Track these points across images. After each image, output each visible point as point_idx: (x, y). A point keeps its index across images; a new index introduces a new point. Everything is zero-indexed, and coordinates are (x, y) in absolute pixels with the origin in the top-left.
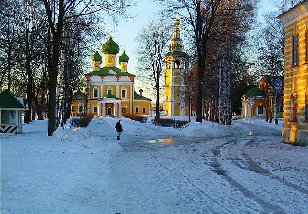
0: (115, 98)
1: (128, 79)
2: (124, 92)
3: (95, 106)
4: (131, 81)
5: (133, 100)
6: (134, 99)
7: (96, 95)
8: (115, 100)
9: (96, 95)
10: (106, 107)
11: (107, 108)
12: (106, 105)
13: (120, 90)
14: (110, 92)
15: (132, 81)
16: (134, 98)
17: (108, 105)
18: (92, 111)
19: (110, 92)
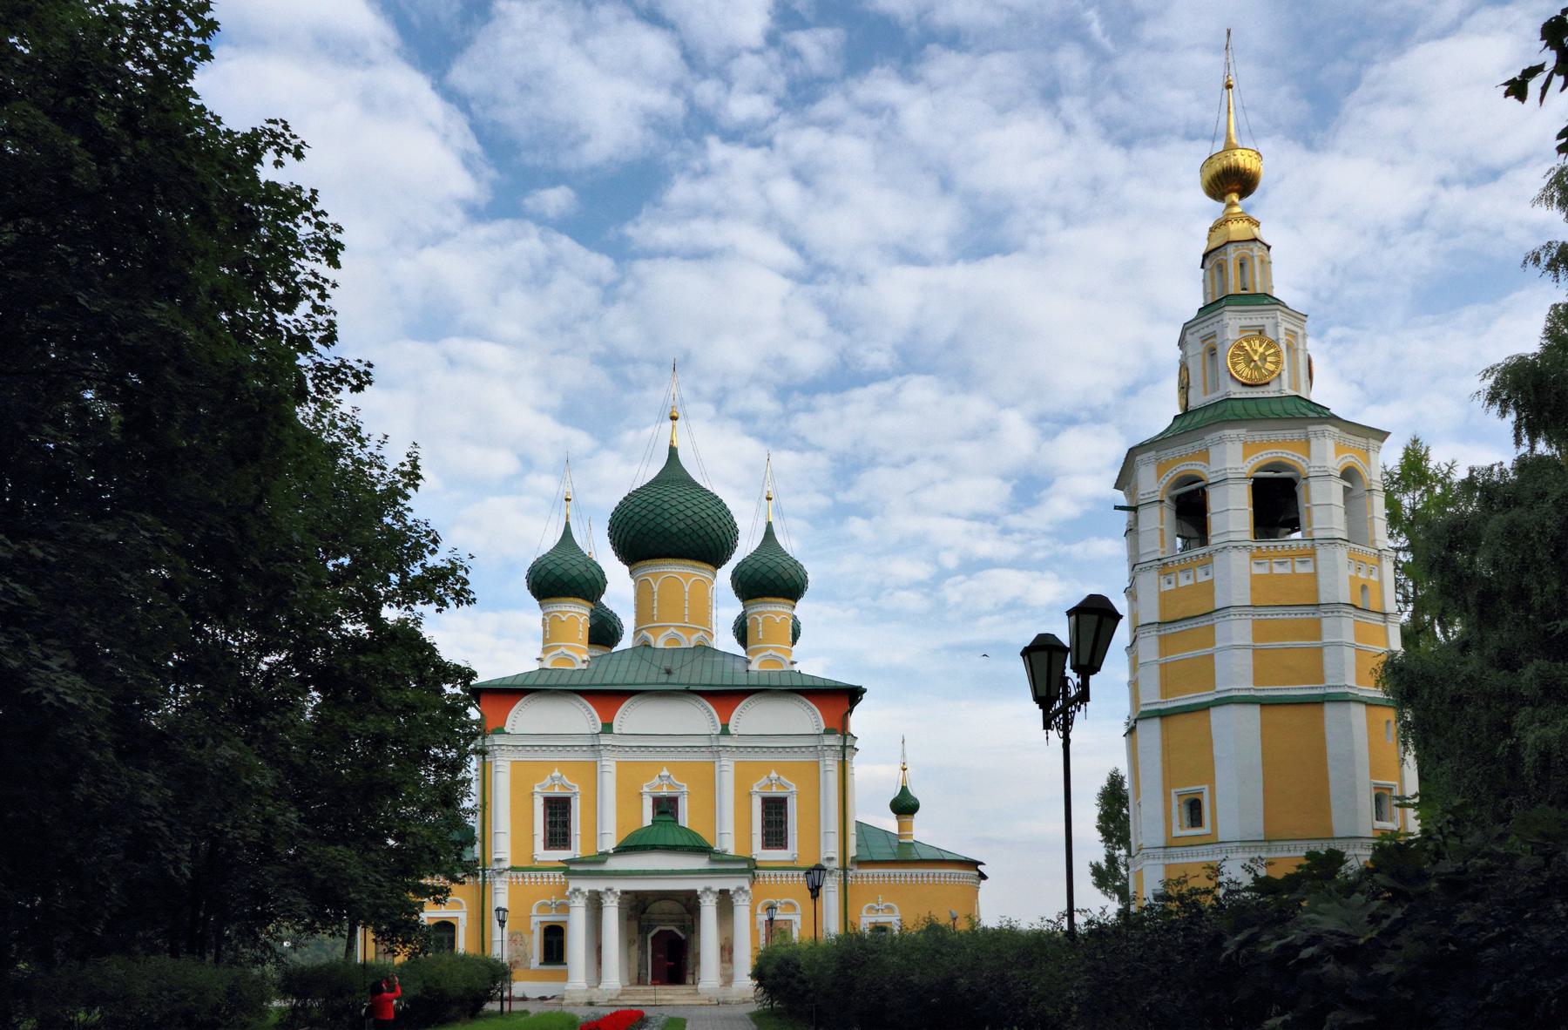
0: (702, 849)
1: (804, 719)
2: (775, 809)
3: (553, 918)
4: (828, 732)
5: (845, 869)
6: (852, 858)
7: (558, 834)
8: (700, 862)
9: (558, 834)
10: (635, 924)
11: (643, 930)
12: (638, 908)
13: (743, 796)
14: (666, 807)
15: (839, 727)
16: (852, 852)
17: (656, 907)
18: (526, 957)
19: (666, 807)
